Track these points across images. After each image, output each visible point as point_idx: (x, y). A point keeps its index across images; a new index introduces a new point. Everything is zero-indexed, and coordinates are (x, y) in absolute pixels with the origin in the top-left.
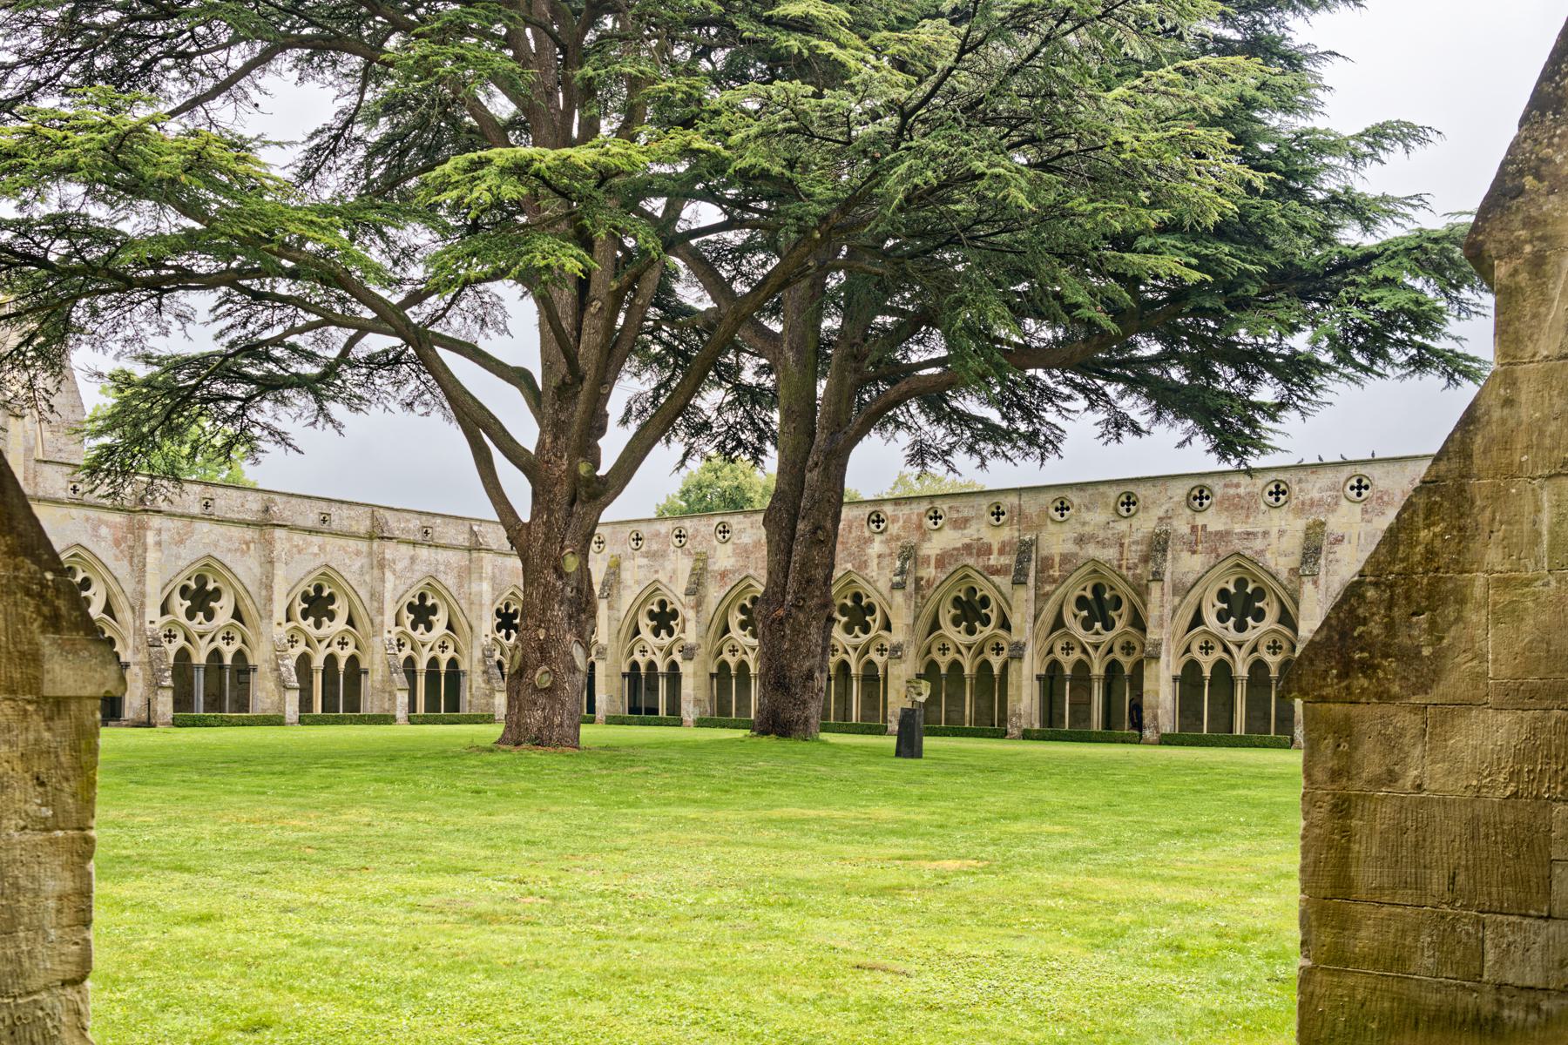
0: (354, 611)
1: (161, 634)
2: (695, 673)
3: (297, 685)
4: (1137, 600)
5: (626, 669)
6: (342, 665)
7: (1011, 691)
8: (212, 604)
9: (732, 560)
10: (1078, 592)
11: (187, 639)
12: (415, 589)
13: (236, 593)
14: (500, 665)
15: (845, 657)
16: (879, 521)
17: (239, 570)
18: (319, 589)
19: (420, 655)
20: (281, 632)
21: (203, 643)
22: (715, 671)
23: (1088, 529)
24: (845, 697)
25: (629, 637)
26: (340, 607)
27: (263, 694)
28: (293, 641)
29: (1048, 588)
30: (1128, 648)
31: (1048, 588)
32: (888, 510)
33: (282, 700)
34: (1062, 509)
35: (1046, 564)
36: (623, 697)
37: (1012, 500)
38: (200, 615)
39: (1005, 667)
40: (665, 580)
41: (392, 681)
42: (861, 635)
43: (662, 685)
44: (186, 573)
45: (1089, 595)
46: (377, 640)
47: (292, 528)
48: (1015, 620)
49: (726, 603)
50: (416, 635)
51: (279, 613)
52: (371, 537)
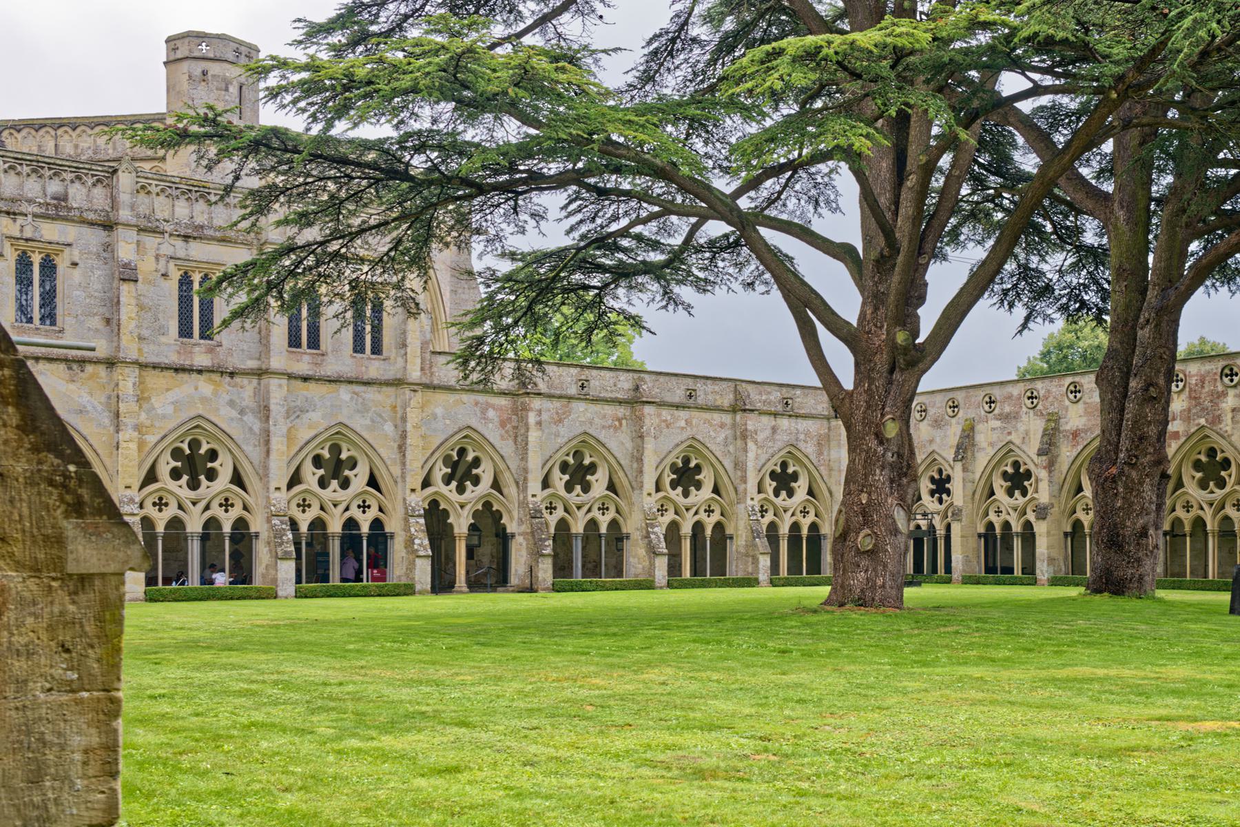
0: (719, 481)
1: (543, 507)
2: (1048, 533)
3: (665, 551)
5: (981, 530)
6: (708, 532)
8: (589, 477)
9: (1084, 420)
11: (566, 510)
12: (776, 457)
13: (610, 466)
15: (1200, 513)
17: (613, 445)
18: (686, 460)
19: (782, 520)
20: (650, 502)
21: (580, 514)
22: (1069, 529)
24: (1200, 555)
25: (984, 498)
26: (706, 477)
27: (635, 559)
28: (662, 510)
33: (652, 566)
36: (979, 557)
38: (578, 488)
40: (1017, 441)
41: (755, 546)
42: (1216, 490)
43: (1017, 544)
44: (565, 449)
46: (742, 506)
47: (661, 404)
49: (1078, 462)
51: (649, 484)
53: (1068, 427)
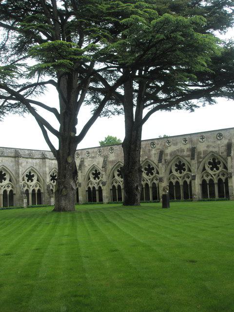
4: (225, 163)
6: (8, 193)
7: (193, 189)
9: (114, 158)
10: (209, 161)
14: (52, 190)
16: (154, 144)
22: (111, 188)
23: (210, 144)
29: (201, 160)
30: (223, 175)
31: (201, 160)
32: (156, 141)
34: (202, 138)
35: (199, 153)
37: (189, 137)
39: (191, 182)
43: (97, 193)
45: (212, 161)
48: (192, 168)
50: (28, 183)
52: (15, 157)
53: (110, 160)
